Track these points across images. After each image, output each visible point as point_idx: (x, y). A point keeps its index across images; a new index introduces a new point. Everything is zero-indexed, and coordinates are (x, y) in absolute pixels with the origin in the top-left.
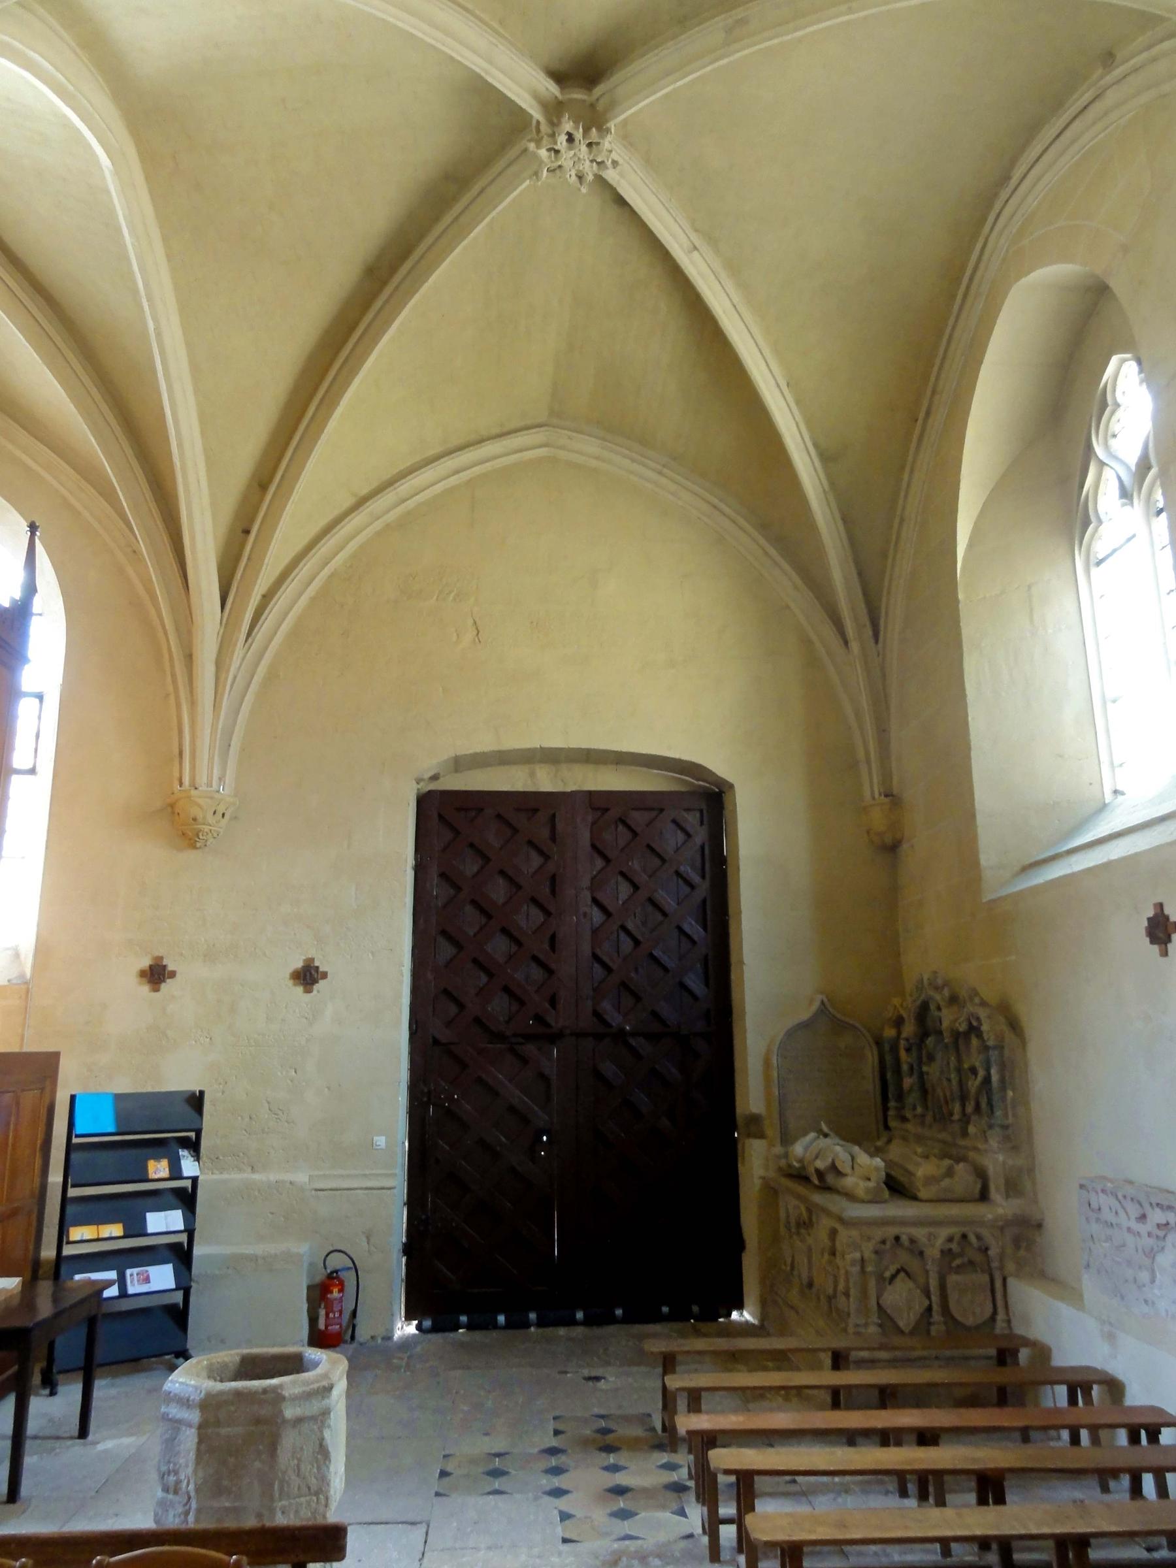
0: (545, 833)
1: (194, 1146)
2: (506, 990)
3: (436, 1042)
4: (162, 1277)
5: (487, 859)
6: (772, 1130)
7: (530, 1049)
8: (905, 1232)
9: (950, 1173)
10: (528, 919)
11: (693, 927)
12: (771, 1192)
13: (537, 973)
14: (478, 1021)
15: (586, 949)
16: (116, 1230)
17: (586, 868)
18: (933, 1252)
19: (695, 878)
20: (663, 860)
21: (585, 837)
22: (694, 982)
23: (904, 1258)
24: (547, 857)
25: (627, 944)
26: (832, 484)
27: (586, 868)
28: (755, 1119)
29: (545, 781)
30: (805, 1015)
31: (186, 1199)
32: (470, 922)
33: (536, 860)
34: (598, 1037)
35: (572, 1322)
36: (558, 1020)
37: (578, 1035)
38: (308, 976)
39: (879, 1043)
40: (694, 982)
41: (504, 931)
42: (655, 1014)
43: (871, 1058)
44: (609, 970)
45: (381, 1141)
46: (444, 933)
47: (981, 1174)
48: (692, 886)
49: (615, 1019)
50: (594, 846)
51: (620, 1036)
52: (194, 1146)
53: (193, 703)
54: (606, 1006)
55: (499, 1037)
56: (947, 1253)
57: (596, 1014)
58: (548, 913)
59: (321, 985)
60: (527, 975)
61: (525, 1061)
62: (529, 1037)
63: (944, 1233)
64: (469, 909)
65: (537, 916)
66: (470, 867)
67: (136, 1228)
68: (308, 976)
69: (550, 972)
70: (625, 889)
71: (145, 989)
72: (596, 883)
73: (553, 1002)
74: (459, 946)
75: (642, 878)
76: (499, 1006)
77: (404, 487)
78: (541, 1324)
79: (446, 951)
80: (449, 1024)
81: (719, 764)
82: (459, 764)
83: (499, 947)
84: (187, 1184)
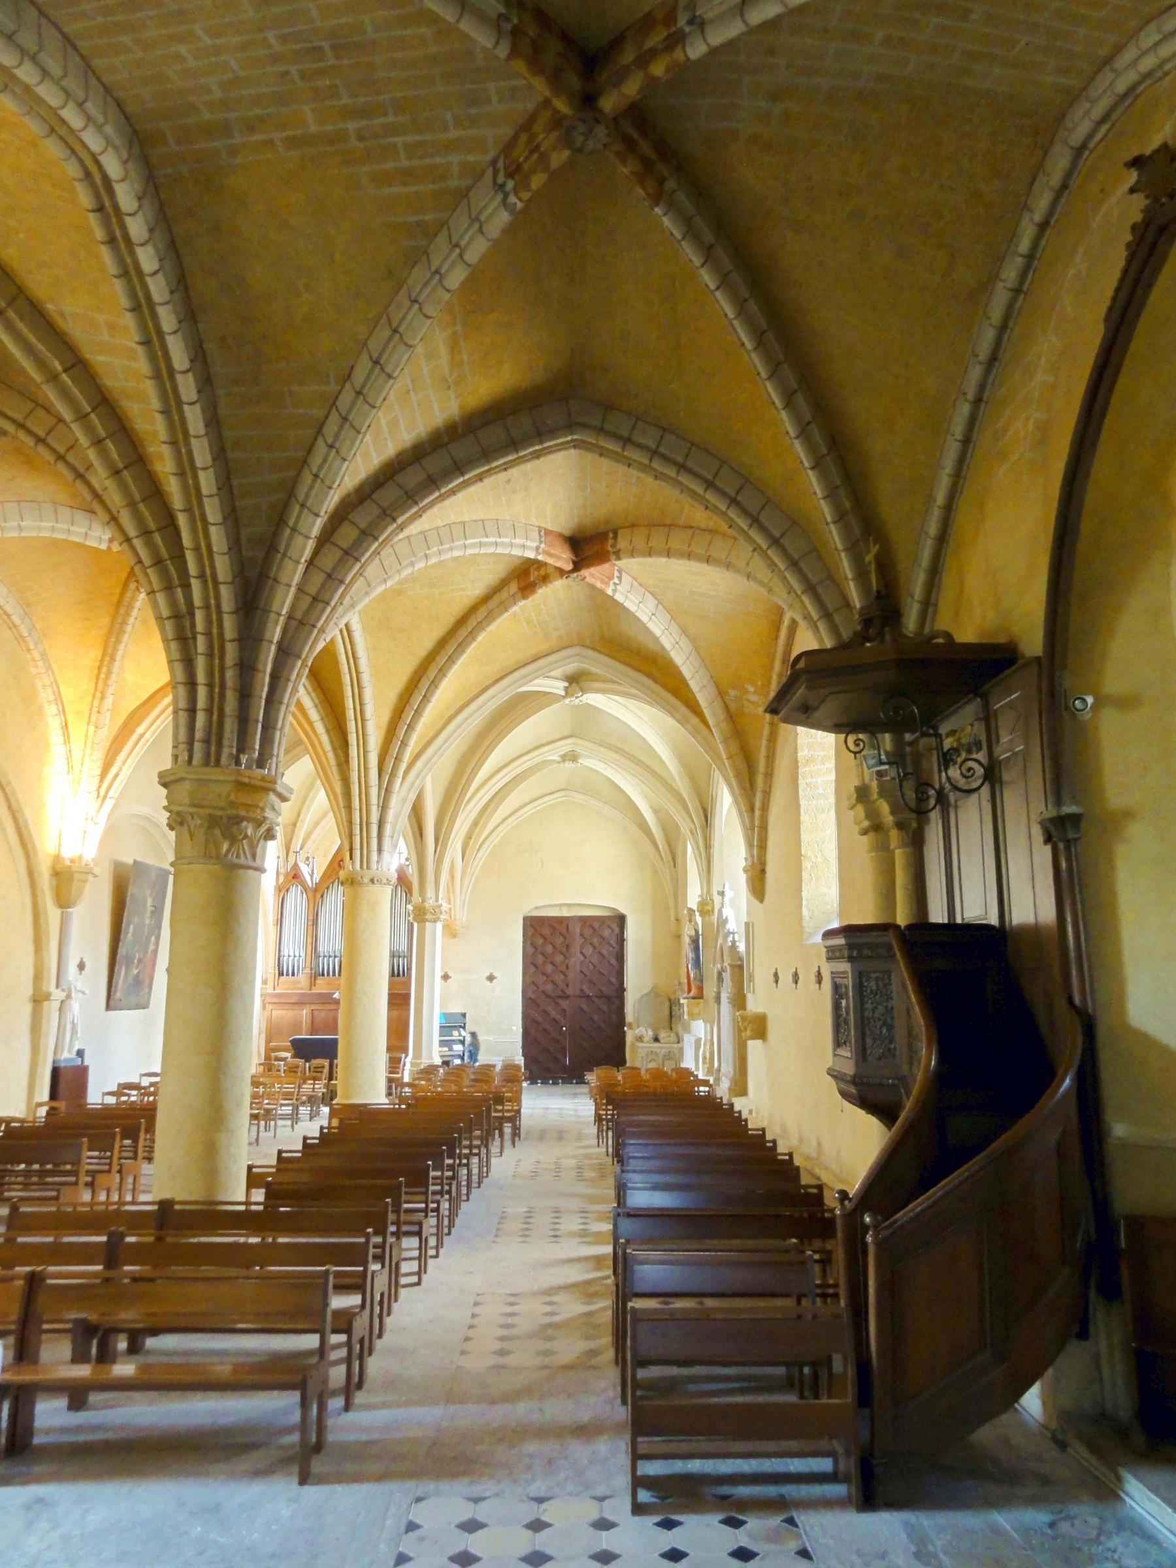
1: (464, 1028)
3: (530, 998)
4: (458, 1062)
6: (635, 1026)
7: (560, 1001)
8: (654, 1050)
9: (669, 1036)
10: (559, 959)
11: (613, 961)
12: (633, 1044)
13: (562, 977)
14: (543, 992)
16: (446, 1049)
17: (578, 941)
18: (661, 1055)
20: (603, 938)
21: (578, 930)
22: (613, 980)
24: (565, 938)
26: (658, 819)
27: (578, 941)
28: (630, 1024)
30: (646, 991)
32: (540, 958)
33: (562, 939)
34: (580, 997)
35: (571, 1083)
36: (570, 991)
38: (491, 978)
39: (670, 1000)
40: (613, 980)
41: (552, 963)
42: (600, 990)
43: (667, 1004)
44: (585, 976)
45: (514, 1028)
49: (587, 992)
50: (581, 935)
51: (588, 997)
52: (464, 1028)
54: (584, 987)
55: (548, 996)
56: (664, 1056)
57: (582, 990)
58: (565, 956)
59: (495, 981)
60: (559, 978)
63: (664, 1050)
64: (540, 956)
66: (540, 941)
67: (451, 1049)
68: (491, 978)
69: (566, 976)
70: (591, 949)
72: (582, 947)
73: (567, 985)
74: (536, 967)
75: (596, 945)
77: (518, 814)
78: (563, 1083)
79: (532, 969)
81: (623, 911)
82: (536, 908)
83: (549, 969)
84: (461, 1038)
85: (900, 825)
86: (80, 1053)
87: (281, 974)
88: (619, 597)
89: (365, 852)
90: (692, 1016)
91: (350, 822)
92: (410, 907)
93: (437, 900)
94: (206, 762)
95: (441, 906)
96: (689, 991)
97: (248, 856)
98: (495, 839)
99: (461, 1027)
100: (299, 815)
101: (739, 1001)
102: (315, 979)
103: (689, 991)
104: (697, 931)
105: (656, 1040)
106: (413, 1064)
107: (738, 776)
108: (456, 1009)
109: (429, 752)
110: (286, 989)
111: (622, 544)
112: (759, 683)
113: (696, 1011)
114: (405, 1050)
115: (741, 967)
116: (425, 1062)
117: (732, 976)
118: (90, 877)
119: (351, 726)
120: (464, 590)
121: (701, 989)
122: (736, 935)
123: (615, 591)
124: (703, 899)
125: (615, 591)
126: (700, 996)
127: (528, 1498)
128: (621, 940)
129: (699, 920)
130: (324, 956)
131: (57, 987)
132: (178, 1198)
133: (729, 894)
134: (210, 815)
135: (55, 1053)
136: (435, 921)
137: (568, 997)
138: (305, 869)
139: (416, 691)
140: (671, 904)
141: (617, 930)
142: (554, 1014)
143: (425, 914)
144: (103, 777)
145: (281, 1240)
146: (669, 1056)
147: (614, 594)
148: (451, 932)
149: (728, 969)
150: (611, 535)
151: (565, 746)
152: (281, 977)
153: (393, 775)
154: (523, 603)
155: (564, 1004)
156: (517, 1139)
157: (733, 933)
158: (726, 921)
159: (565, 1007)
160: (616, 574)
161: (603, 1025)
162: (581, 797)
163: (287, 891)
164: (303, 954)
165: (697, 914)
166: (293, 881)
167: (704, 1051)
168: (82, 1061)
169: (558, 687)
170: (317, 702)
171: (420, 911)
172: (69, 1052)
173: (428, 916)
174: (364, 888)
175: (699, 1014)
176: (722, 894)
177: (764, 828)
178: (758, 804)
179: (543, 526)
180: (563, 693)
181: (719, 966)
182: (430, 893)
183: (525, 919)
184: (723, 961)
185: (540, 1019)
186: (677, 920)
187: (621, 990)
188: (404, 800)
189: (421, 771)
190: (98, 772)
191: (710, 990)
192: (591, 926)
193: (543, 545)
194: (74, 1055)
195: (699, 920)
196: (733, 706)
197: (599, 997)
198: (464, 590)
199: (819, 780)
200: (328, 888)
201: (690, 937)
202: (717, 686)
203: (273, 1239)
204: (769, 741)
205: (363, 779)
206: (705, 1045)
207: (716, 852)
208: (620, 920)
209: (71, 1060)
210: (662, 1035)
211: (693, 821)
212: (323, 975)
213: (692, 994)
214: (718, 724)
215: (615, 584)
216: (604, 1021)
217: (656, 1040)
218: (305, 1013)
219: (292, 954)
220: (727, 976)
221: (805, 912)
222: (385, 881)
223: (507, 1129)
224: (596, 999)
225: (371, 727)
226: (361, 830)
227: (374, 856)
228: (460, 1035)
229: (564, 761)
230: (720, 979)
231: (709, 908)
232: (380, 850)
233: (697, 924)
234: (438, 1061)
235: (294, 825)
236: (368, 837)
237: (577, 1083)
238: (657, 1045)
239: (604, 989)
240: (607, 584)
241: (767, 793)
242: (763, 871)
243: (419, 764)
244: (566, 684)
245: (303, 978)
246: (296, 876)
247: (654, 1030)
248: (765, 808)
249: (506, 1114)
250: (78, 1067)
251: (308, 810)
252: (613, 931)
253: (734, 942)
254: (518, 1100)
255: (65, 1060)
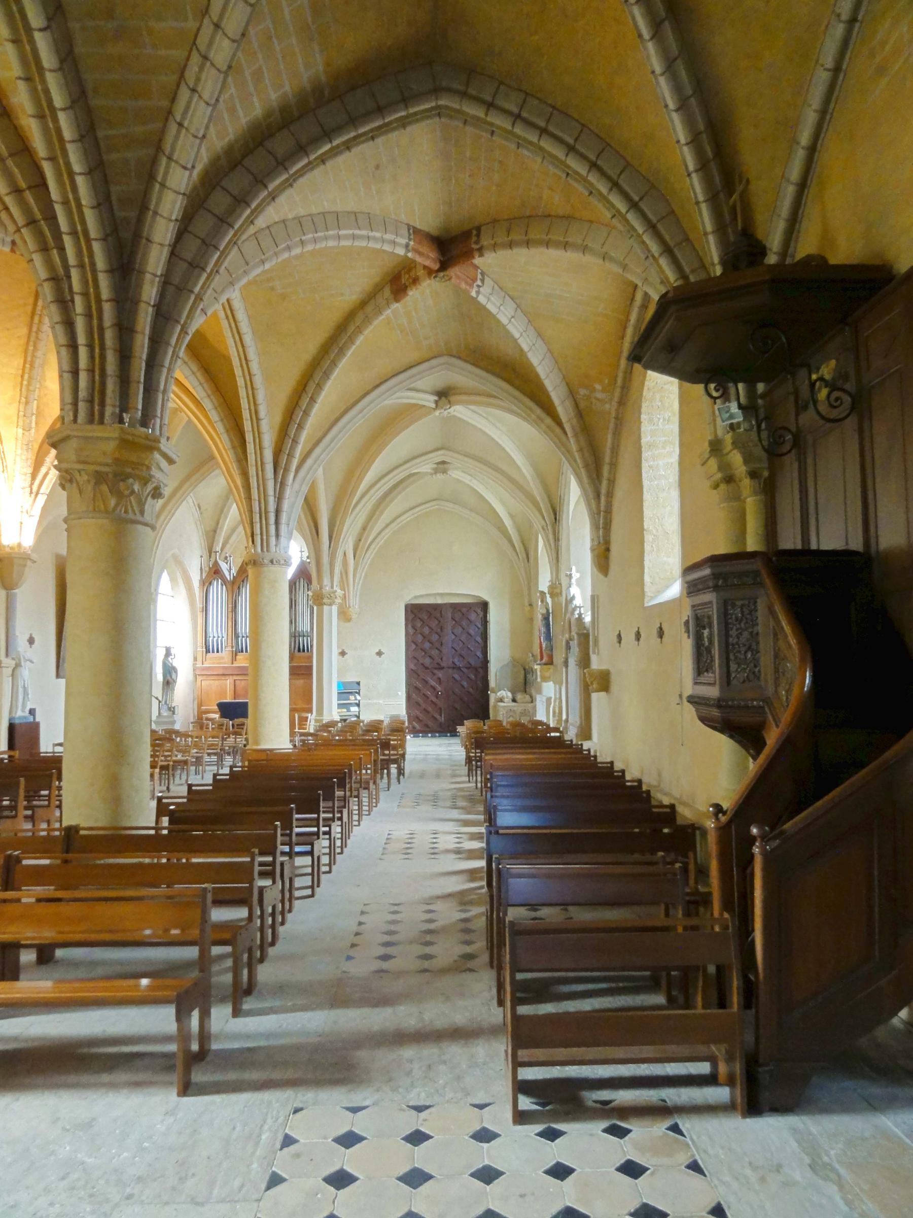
0: (439, 615)
1: (359, 693)
2: (430, 656)
5: (424, 622)
7: (436, 671)
8: (512, 709)
10: (435, 637)
11: (479, 639)
14: (422, 664)
15: (450, 646)
16: (345, 710)
19: (480, 626)
20: (471, 622)
21: (450, 615)
23: (512, 714)
25: (461, 644)
28: (493, 688)
29: (439, 601)
30: (506, 662)
31: (358, 705)
34: (454, 668)
35: (447, 736)
36: (443, 664)
37: (449, 668)
39: (525, 669)
41: (429, 641)
43: (523, 672)
45: (400, 693)
46: (413, 642)
47: (531, 697)
48: (479, 628)
49: (458, 664)
51: (459, 668)
52: (359, 693)
53: (348, 585)
54: (456, 660)
55: (427, 668)
57: (453, 663)
61: (434, 674)
62: (436, 669)
65: (437, 637)
67: (349, 711)
68: (379, 654)
69: (441, 651)
70: (460, 629)
71: (341, 657)
72: (453, 627)
76: (427, 661)
77: (399, 520)
79: (414, 646)
80: (415, 665)
82: (416, 597)
83: (427, 645)
84: (357, 702)
85: (753, 475)
86: (32, 712)
87: (208, 651)
88: (482, 299)
89: (265, 537)
90: (545, 679)
91: (251, 511)
92: (310, 593)
93: (332, 587)
94: (91, 420)
95: (336, 591)
96: (542, 659)
97: (138, 513)
98: (381, 541)
99: (356, 693)
100: (218, 523)
101: (585, 662)
102: (236, 655)
103: (542, 659)
104: (548, 610)
105: (514, 700)
106: (316, 721)
107: (586, 466)
108: (351, 678)
109: (318, 450)
110: (213, 663)
111: (485, 241)
112: (606, 381)
113: (547, 674)
114: (310, 710)
115: (587, 636)
116: (326, 719)
117: (579, 644)
118: (29, 563)
119: (247, 426)
120: (342, 294)
121: (551, 657)
122: (582, 609)
123: (478, 293)
124: (552, 583)
125: (478, 293)
126: (550, 662)
127: (408, 1106)
128: (485, 622)
129: (549, 600)
130: (243, 637)
131: (7, 655)
132: (83, 825)
133: (576, 575)
134: (97, 472)
135: (10, 712)
136: (331, 605)
137: (442, 668)
138: (224, 566)
139: (304, 394)
140: (526, 592)
141: (481, 614)
142: (433, 683)
143: (322, 598)
144: (34, 476)
145: (194, 860)
146: (524, 713)
147: (478, 296)
148: (344, 615)
149: (576, 637)
150: (474, 232)
151: (438, 456)
152: (208, 654)
153: (286, 470)
154: (395, 306)
155: (440, 674)
156: (402, 777)
157: (580, 607)
158: (573, 598)
159: (440, 675)
160: (479, 276)
161: (471, 690)
162: (451, 505)
163: (210, 584)
164: (225, 635)
165: (548, 596)
166: (215, 576)
167: (554, 708)
168: (34, 719)
169: (429, 400)
170: (210, 392)
171: (318, 596)
172: (23, 711)
173: (325, 601)
174: (266, 569)
175: (550, 677)
176: (570, 576)
177: (608, 511)
178: (603, 490)
179: (412, 223)
180: (433, 406)
181: (567, 636)
182: (326, 581)
183: (407, 606)
184: (570, 632)
185: (420, 686)
186: (530, 605)
187: (485, 662)
188: (298, 492)
189: (310, 468)
190: (30, 470)
191: (559, 657)
192: (460, 611)
193: (412, 243)
194: (27, 713)
195: (549, 600)
196: (582, 405)
197: (466, 668)
198: (342, 294)
199: (661, 463)
200: (243, 581)
201: (543, 615)
202: (567, 384)
203: (187, 860)
204: (614, 434)
205: (260, 473)
206: (555, 701)
207: (563, 543)
208: (484, 606)
209: (25, 717)
210: (519, 697)
211: (544, 518)
212: (242, 651)
213: (544, 661)
214: (569, 420)
215: (479, 286)
216: (472, 688)
217: (514, 700)
218: (229, 682)
219: (216, 635)
220: (574, 644)
221: (647, 579)
222: (282, 562)
223: (393, 769)
224: (465, 670)
225: (265, 425)
226: (261, 518)
227: (273, 540)
228: (356, 699)
229: (436, 473)
230: (568, 647)
231: (558, 591)
232: (277, 535)
233: (547, 603)
234: (337, 718)
235: (215, 531)
236: (267, 524)
237: (451, 736)
238: (514, 704)
239: (473, 663)
240: (471, 286)
241: (612, 482)
242: (608, 550)
243: (309, 462)
244: (436, 398)
245: (226, 654)
246: (216, 572)
247: (513, 693)
248: (610, 495)
249: (392, 757)
250: (30, 723)
251: (226, 518)
252: (478, 615)
253: (580, 615)
254: (403, 746)
255: (20, 718)
